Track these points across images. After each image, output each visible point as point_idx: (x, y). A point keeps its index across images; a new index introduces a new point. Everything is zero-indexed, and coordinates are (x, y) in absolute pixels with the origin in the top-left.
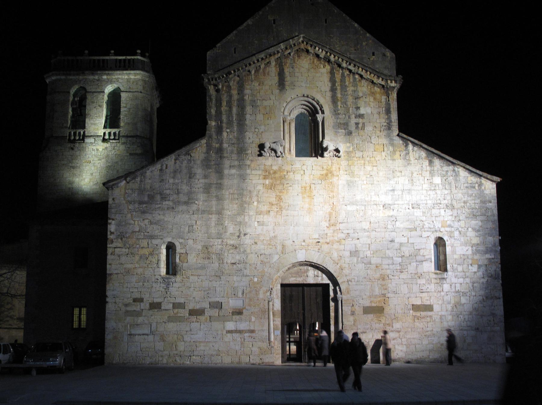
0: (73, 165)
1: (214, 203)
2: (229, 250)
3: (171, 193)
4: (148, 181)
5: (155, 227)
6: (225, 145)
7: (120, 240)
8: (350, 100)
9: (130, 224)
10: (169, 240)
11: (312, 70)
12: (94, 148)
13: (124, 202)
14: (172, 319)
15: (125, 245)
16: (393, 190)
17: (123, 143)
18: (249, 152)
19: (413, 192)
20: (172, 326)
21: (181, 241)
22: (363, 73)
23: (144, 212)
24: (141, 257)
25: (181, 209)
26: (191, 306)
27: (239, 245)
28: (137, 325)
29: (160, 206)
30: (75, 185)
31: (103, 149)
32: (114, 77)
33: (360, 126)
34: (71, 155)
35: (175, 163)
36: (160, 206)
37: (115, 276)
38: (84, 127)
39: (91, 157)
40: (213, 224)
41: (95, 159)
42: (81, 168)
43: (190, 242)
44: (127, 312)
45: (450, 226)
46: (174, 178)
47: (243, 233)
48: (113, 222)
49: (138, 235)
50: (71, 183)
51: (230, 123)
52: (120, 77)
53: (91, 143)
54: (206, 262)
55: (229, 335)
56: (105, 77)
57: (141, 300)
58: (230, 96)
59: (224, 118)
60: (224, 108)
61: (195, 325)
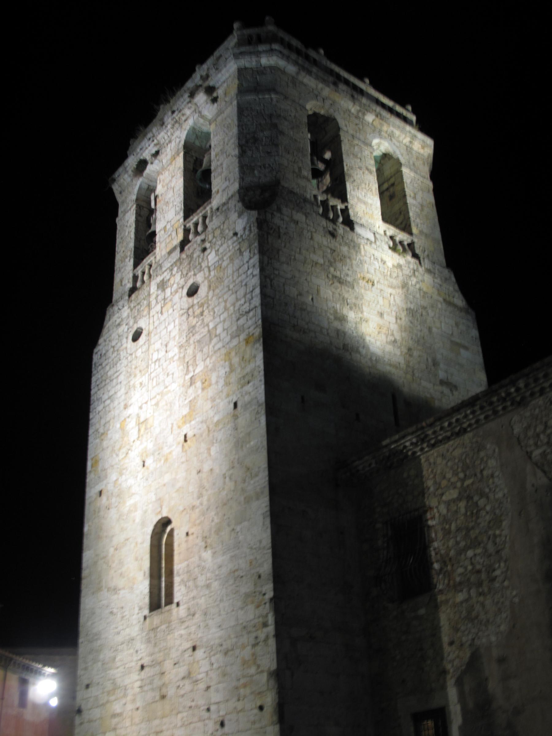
0: (338, 274)
12: (377, 254)
17: (429, 271)
30: (350, 326)
32: (385, 128)
34: (331, 249)
38: (344, 198)
39: (373, 271)
42: (356, 288)
50: (342, 319)
52: (397, 133)
53: (368, 239)
56: (370, 118)
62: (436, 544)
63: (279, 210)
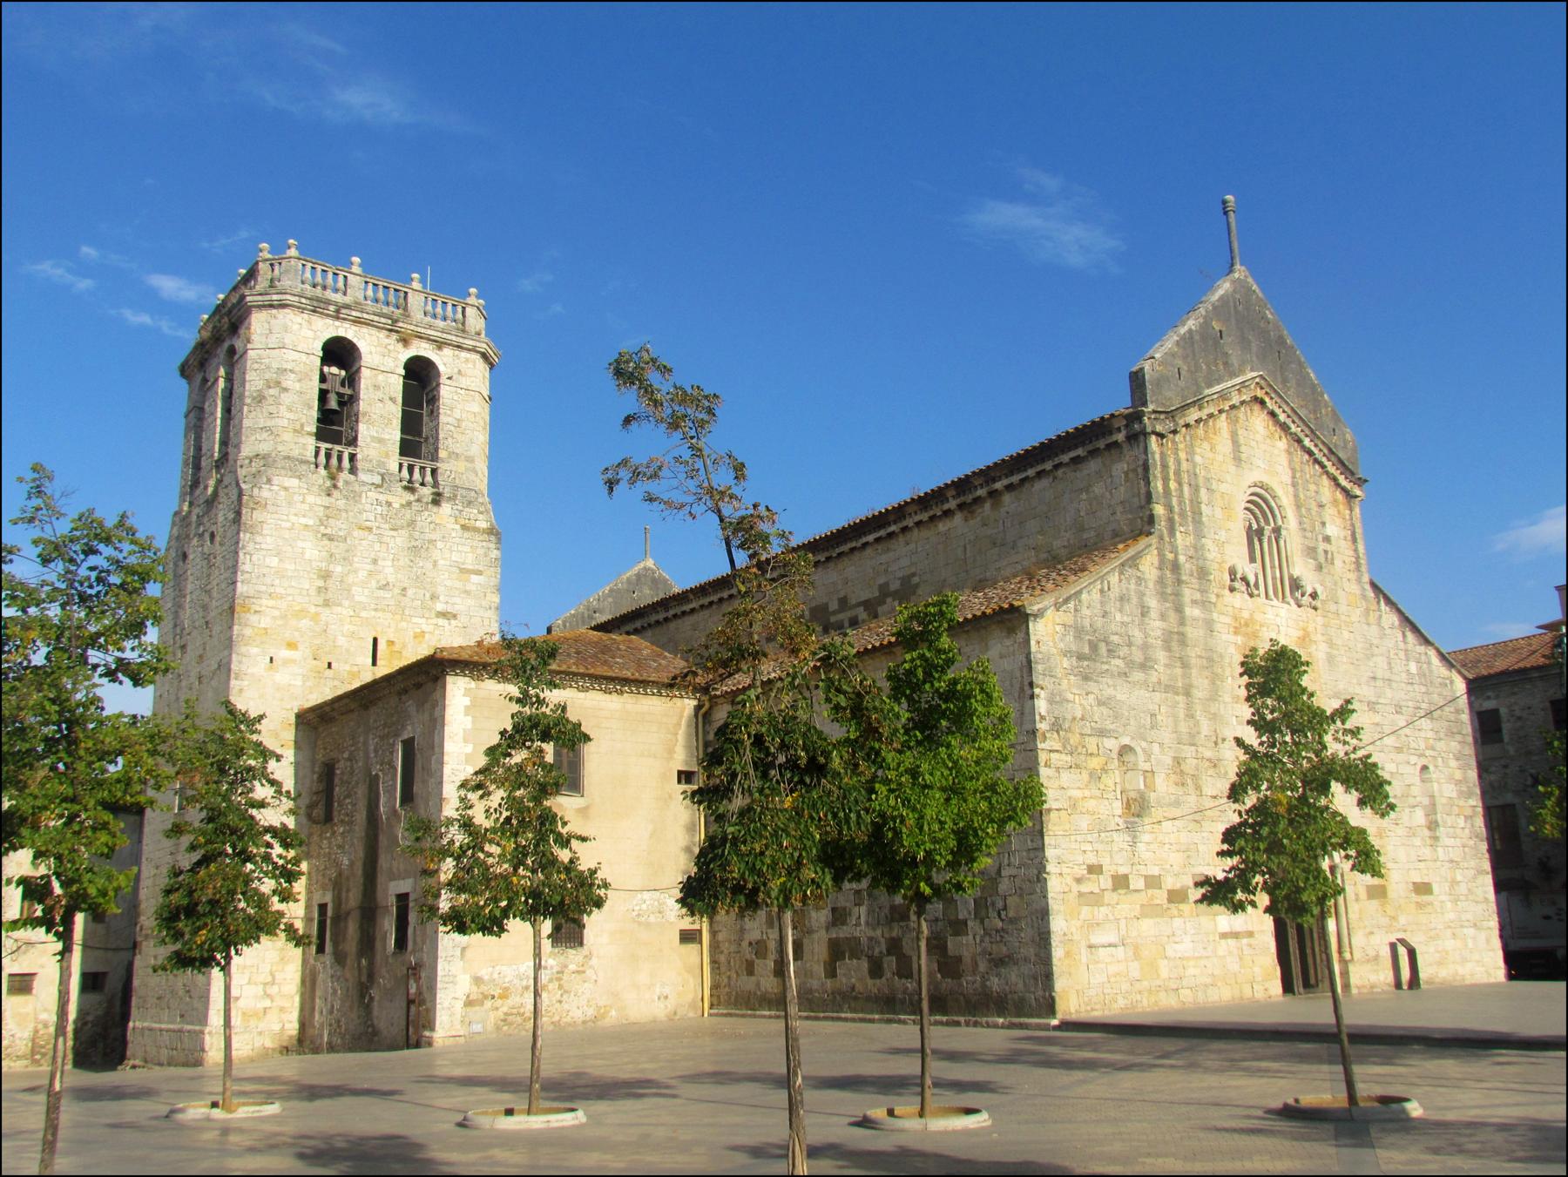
1: (1179, 671)
2: (1206, 769)
3: (1121, 642)
4: (1085, 612)
5: (1104, 710)
6: (1182, 559)
7: (1055, 734)
8: (1313, 506)
9: (1068, 701)
10: (1126, 741)
11: (1268, 441)
13: (1055, 651)
14: (1149, 910)
15: (1065, 747)
16: (1374, 678)
18: (1212, 577)
19: (1394, 685)
20: (1147, 926)
21: (1144, 744)
22: (1327, 463)
23: (1086, 678)
24: (1091, 775)
25: (1136, 679)
26: (1170, 883)
27: (1219, 760)
28: (1098, 924)
29: (1105, 667)
31: (402, 506)
33: (1329, 556)
35: (1120, 581)
36: (1105, 667)
37: (1053, 815)
40: (1182, 715)
41: (383, 526)
43: (1156, 747)
44: (1081, 894)
45: (1433, 749)
46: (1121, 611)
47: (1220, 736)
48: (1043, 694)
49: (1082, 728)
51: (1182, 514)
54: (1180, 791)
55: (1223, 941)
57: (1094, 869)
58: (1178, 462)
59: (1175, 501)
60: (1173, 485)
61: (1177, 922)
62: (337, 789)
63: (269, 481)
